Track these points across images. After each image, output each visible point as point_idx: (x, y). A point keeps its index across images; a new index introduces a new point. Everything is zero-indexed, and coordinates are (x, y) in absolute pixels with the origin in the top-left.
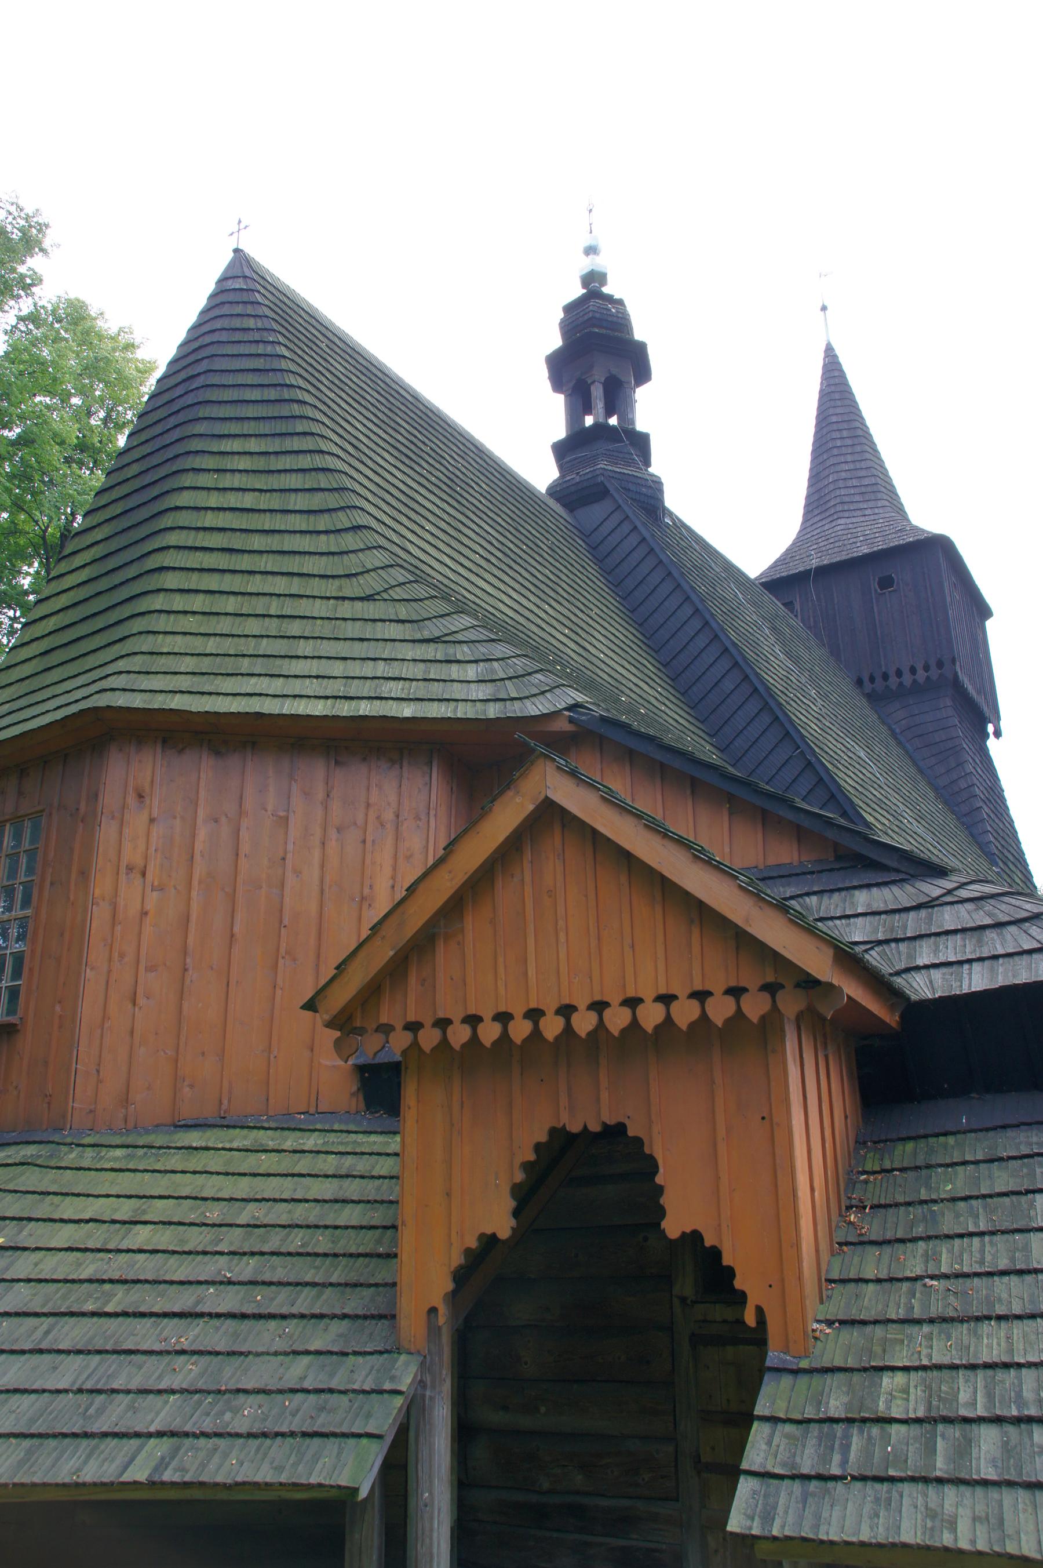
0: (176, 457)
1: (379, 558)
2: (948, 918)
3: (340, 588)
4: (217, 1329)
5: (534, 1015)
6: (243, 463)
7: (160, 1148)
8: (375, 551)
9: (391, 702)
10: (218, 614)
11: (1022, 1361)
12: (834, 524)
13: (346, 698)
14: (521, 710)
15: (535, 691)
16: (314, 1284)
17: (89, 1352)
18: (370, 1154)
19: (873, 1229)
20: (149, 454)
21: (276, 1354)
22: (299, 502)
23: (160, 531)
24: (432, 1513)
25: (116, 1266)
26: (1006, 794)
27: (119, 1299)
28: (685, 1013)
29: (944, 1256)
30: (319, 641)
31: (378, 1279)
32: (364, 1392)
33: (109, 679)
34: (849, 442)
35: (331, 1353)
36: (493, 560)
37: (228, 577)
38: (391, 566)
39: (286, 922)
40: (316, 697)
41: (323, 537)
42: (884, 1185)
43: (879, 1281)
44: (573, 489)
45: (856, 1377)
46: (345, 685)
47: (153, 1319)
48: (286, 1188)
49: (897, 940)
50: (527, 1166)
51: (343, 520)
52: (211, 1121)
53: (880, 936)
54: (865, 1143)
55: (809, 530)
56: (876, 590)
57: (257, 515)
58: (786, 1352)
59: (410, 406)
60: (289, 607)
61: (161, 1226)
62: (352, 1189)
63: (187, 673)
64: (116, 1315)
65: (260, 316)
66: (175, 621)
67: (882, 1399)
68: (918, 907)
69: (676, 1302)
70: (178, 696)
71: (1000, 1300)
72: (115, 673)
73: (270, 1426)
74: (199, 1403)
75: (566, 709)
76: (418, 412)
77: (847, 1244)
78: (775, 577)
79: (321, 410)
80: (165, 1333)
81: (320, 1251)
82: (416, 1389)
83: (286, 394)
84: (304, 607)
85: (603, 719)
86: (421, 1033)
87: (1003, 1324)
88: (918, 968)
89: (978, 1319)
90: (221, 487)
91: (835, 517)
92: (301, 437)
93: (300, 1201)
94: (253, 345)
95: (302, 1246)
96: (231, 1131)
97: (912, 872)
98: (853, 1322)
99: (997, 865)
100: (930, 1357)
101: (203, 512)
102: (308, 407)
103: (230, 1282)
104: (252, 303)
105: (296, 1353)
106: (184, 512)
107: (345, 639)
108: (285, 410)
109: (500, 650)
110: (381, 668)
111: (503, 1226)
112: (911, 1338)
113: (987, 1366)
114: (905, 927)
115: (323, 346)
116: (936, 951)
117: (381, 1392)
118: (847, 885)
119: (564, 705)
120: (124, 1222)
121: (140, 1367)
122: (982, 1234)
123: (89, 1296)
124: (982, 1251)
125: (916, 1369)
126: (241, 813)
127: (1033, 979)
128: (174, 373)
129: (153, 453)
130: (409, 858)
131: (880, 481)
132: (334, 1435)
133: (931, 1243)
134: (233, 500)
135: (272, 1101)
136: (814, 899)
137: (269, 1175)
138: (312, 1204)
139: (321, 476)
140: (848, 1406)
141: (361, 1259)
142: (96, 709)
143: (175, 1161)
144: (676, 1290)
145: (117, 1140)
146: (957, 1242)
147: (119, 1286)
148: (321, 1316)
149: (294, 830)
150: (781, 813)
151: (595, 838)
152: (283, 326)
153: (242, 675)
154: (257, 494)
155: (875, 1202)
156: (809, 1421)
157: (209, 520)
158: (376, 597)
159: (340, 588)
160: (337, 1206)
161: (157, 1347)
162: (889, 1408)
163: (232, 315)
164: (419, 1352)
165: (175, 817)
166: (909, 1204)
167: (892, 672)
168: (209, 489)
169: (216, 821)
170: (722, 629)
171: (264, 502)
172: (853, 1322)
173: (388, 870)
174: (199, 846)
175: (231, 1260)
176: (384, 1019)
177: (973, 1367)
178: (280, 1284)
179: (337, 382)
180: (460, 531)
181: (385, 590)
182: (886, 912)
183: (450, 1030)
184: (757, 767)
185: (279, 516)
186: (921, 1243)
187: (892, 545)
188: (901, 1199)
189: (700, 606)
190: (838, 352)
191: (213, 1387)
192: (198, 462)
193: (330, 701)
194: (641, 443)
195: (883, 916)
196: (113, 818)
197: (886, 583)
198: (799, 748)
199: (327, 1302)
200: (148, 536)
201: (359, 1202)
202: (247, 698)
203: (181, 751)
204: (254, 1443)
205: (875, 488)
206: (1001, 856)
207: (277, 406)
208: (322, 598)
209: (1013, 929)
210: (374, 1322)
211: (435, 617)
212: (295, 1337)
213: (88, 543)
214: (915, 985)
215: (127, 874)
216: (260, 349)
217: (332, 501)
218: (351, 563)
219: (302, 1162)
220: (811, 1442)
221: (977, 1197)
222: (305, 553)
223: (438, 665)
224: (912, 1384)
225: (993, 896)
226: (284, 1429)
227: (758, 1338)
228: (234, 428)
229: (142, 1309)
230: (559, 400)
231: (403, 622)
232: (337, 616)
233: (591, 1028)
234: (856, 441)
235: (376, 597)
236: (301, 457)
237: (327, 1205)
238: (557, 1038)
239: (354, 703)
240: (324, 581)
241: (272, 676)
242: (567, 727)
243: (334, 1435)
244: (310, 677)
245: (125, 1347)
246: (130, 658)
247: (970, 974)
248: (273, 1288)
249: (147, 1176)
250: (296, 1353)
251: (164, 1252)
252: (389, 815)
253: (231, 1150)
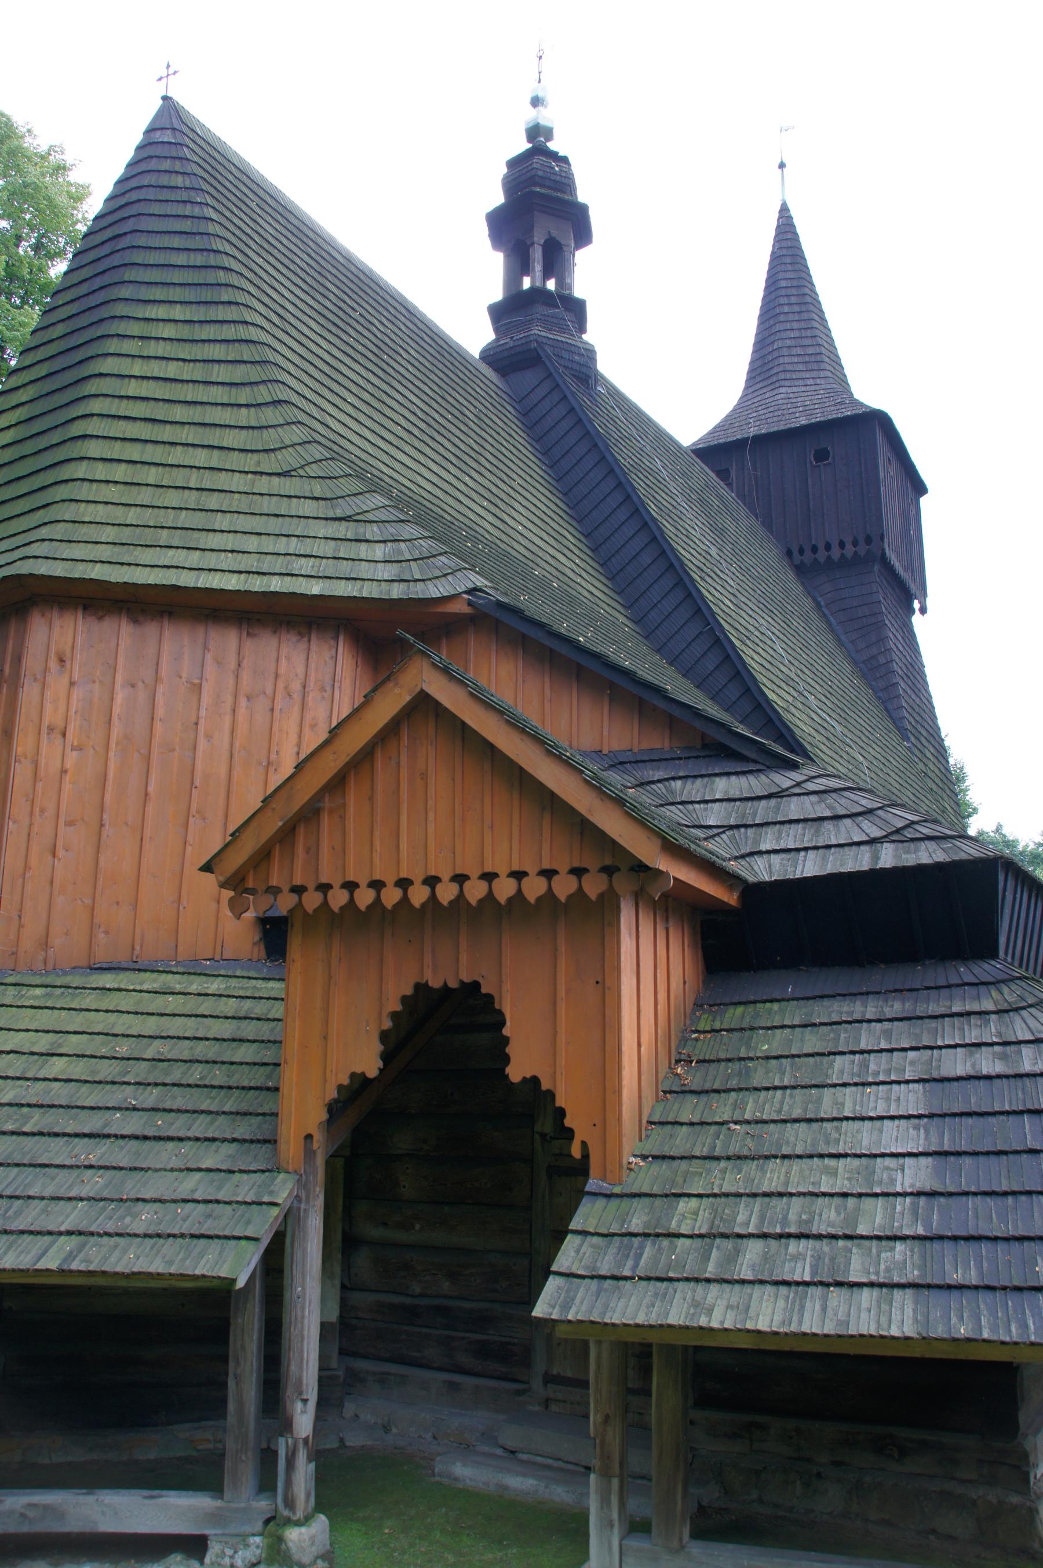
0: (102, 320)
1: (297, 434)
2: (794, 808)
3: (258, 463)
4: (122, 1148)
5: (404, 884)
6: (168, 331)
7: (76, 988)
8: (294, 427)
9: (301, 579)
10: (139, 484)
11: (794, 1191)
12: (775, 392)
13: (258, 573)
14: (423, 592)
15: (438, 573)
16: (210, 1112)
17: (9, 1165)
18: (268, 999)
19: (694, 1079)
20: (74, 315)
21: (172, 1170)
22: (221, 373)
23: (85, 397)
24: (304, 1304)
25: (34, 1092)
26: (927, 670)
27: (35, 1121)
28: (534, 888)
29: (750, 1105)
30: (236, 515)
31: (266, 1109)
32: (246, 1203)
33: (32, 545)
34: (796, 309)
35: (220, 1170)
36: (416, 432)
37: (150, 447)
38: (309, 442)
39: (197, 782)
40: (230, 571)
41: (244, 411)
42: (712, 1043)
43: (692, 1124)
44: (506, 354)
45: (658, 1202)
46: (258, 561)
47: (66, 1138)
48: (190, 1026)
49: (746, 826)
50: (394, 1016)
51: (264, 394)
52: (124, 965)
53: (732, 822)
54: (702, 1006)
55: (750, 397)
56: (811, 462)
57: (180, 385)
58: (604, 1179)
59: (341, 268)
60: (208, 480)
61: (75, 1058)
62: (249, 1030)
63: (107, 543)
64: (33, 1134)
65: (188, 174)
66: (97, 490)
67: (675, 1219)
68: (769, 796)
69: (537, 1137)
70: (98, 565)
71: (787, 1143)
72: (38, 541)
73: (163, 1229)
74: (104, 1209)
75: (465, 592)
76: (349, 275)
77: (671, 1092)
78: (712, 444)
79: (247, 278)
80: (75, 1151)
81: (216, 1083)
82: (292, 1203)
83: (213, 260)
84: (222, 481)
85: (500, 604)
86: (305, 896)
87: (786, 1162)
88: (760, 853)
89: (767, 1157)
90: (145, 355)
91: (777, 385)
92: (227, 307)
93: (201, 1039)
94: (181, 205)
95: (201, 1079)
96: (142, 974)
97: (768, 764)
98: (664, 1157)
99: (908, 740)
100: (721, 1186)
101: (127, 380)
102: (234, 274)
103: (135, 1109)
104: (180, 158)
105: (189, 1170)
106: (108, 379)
107: (261, 514)
108: (211, 277)
109: (409, 531)
110: (294, 545)
111: (370, 1064)
112: (709, 1171)
113: (766, 1195)
114: (755, 814)
115: (253, 205)
116: (779, 838)
117: (260, 1204)
118: (710, 772)
119: (464, 589)
120: (42, 1054)
121: (53, 1179)
122: (784, 1088)
123: (9, 1117)
124: (782, 1103)
125: (708, 1196)
126: (157, 679)
127: (857, 869)
128: (101, 230)
129: (78, 314)
130: (313, 726)
132: (218, 1237)
133: (741, 1094)
134: (156, 369)
135: (180, 948)
136: (679, 783)
137: (175, 1015)
138: (213, 1042)
139: (244, 347)
140: (646, 1224)
141: (252, 1091)
142: (19, 577)
143: (89, 1000)
144: (538, 1128)
145: (38, 981)
146: (763, 1093)
147: (36, 1109)
148: (214, 1140)
149: (206, 699)
150: (655, 702)
151: (464, 733)
152: (212, 185)
153: (160, 546)
154: (180, 363)
155: (701, 1058)
156: (613, 1235)
157: (133, 388)
158: (293, 473)
159: (258, 463)
160: (235, 1044)
161: (68, 1162)
162: (679, 1226)
163: (159, 171)
164: (296, 1172)
165: (94, 682)
166: (729, 1060)
167: (821, 546)
168: (133, 356)
169: (133, 686)
170: (642, 503)
171: (187, 372)
172: (664, 1157)
173: (293, 738)
174: (117, 710)
175: (137, 1089)
176: (274, 882)
177: (754, 1195)
178: (179, 1111)
179: (265, 245)
180: (383, 403)
181: (302, 467)
182: (740, 800)
183: (330, 893)
184: (668, 641)
185: (201, 387)
186: (733, 1094)
187: (830, 417)
188: (722, 1055)
189: (623, 480)
190: (793, 213)
191: (116, 1197)
192: (122, 328)
193: (243, 576)
194: (577, 309)
195: (738, 803)
196: (35, 680)
197: (822, 455)
198: (709, 624)
199: (220, 1127)
200: (72, 402)
201: (255, 1041)
202: (165, 569)
203: (100, 618)
204: (149, 1242)
205: (818, 358)
206: (913, 731)
207: (203, 272)
208: (240, 472)
209: (847, 822)
210: (259, 1146)
211: (349, 496)
212: (190, 1156)
213: (13, 404)
214: (756, 868)
215: (48, 734)
216: (188, 210)
217: (254, 373)
218: (270, 438)
219: (205, 1005)
220: (612, 1250)
221: (787, 1057)
222: (226, 426)
223: (349, 543)
224: (702, 1208)
225: (835, 790)
226: (176, 1231)
227: (582, 1169)
228: (158, 293)
229: (56, 1130)
230: (498, 259)
231: (317, 499)
232: (255, 491)
233: (452, 898)
234: (804, 308)
235: (293, 473)
236: (225, 326)
237: (225, 1044)
238: (423, 905)
239: (266, 578)
240: (242, 455)
241: (189, 548)
242: (467, 610)
243: (218, 1237)
244: (225, 551)
245: (40, 1161)
246: (53, 525)
247: (804, 861)
248: (173, 1114)
249: (64, 1013)
250: (189, 1170)
251: (77, 1081)
252: (296, 686)
253: (141, 991)
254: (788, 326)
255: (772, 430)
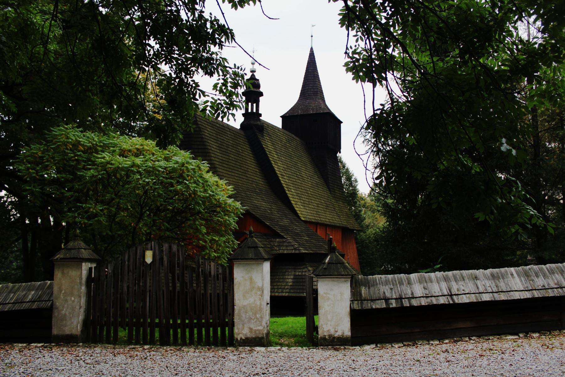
2: (285, 244)
131: (318, 90)
254: (310, 83)
255: (305, 113)
